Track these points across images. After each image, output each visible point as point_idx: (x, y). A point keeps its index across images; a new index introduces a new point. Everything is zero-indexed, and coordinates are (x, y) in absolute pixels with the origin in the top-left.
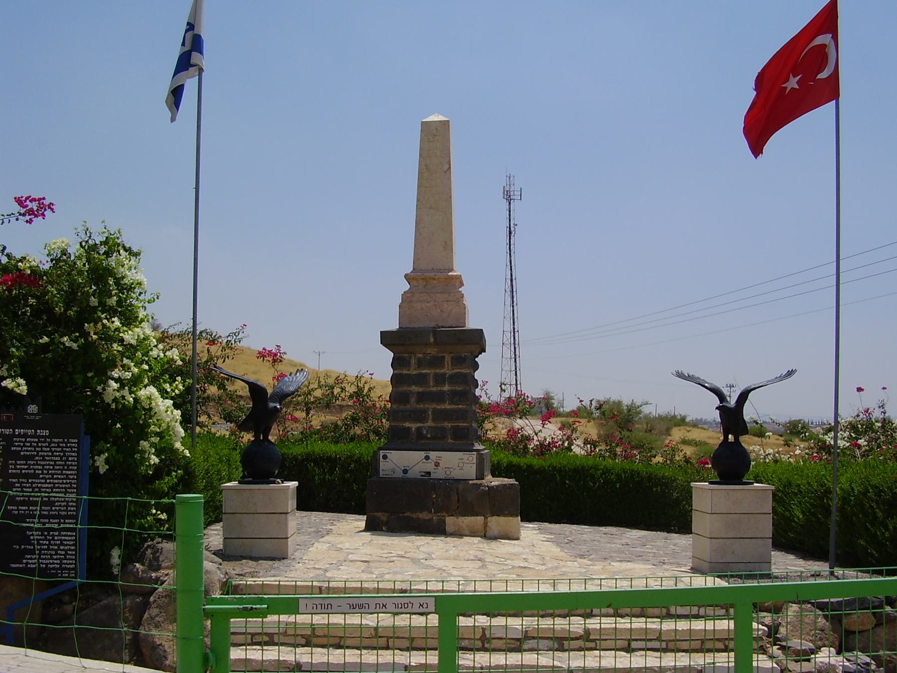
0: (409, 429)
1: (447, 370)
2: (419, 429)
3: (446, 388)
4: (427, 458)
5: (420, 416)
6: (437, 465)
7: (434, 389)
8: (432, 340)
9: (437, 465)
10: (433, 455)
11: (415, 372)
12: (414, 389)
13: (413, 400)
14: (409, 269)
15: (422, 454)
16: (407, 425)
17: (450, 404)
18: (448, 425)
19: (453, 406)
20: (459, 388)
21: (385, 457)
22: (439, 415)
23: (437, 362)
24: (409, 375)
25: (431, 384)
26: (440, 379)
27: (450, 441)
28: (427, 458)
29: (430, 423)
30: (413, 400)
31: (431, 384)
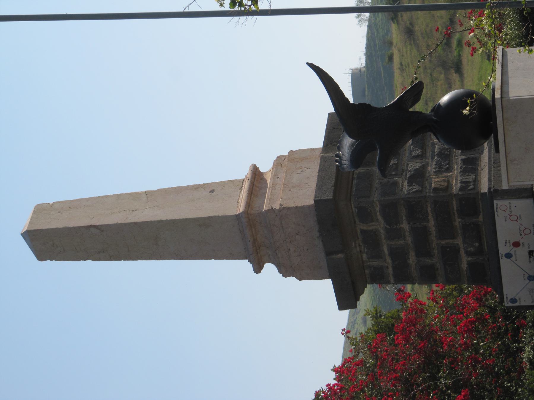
0: (469, 264)
1: (380, 225)
2: (468, 254)
3: (405, 226)
4: (508, 256)
5: (450, 255)
6: (516, 244)
7: (409, 239)
8: (340, 256)
9: (516, 244)
10: (503, 249)
11: (389, 260)
12: (412, 259)
13: (428, 261)
14: (244, 266)
15: (504, 263)
16: (464, 266)
17: (428, 221)
18: (458, 222)
19: (430, 217)
20: (403, 213)
21: (513, 300)
22: (446, 229)
23: (371, 240)
24: (394, 268)
25: (402, 242)
26: (394, 233)
27: (481, 218)
28: (508, 256)
29: (459, 241)
30: (428, 261)
31: (402, 242)
